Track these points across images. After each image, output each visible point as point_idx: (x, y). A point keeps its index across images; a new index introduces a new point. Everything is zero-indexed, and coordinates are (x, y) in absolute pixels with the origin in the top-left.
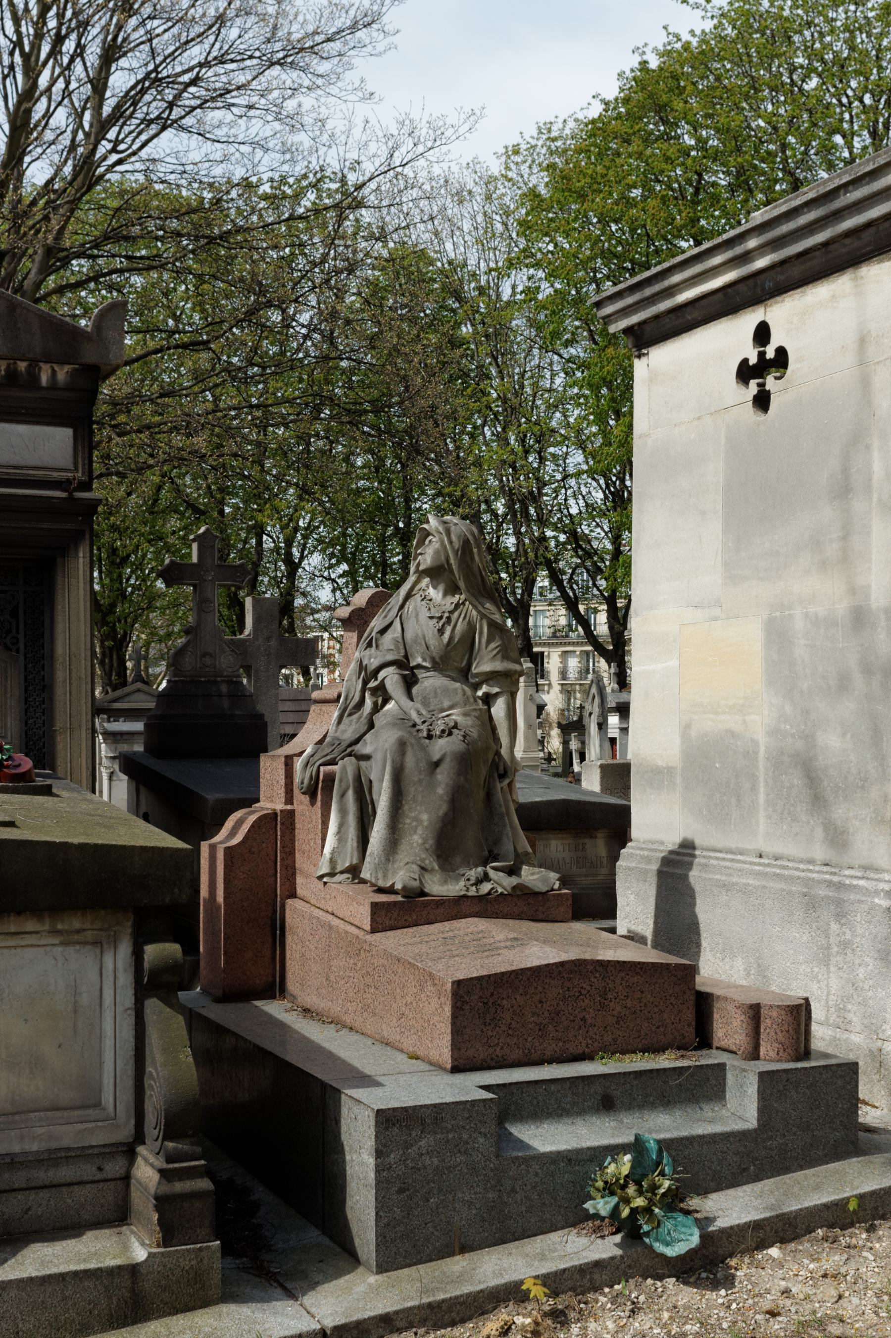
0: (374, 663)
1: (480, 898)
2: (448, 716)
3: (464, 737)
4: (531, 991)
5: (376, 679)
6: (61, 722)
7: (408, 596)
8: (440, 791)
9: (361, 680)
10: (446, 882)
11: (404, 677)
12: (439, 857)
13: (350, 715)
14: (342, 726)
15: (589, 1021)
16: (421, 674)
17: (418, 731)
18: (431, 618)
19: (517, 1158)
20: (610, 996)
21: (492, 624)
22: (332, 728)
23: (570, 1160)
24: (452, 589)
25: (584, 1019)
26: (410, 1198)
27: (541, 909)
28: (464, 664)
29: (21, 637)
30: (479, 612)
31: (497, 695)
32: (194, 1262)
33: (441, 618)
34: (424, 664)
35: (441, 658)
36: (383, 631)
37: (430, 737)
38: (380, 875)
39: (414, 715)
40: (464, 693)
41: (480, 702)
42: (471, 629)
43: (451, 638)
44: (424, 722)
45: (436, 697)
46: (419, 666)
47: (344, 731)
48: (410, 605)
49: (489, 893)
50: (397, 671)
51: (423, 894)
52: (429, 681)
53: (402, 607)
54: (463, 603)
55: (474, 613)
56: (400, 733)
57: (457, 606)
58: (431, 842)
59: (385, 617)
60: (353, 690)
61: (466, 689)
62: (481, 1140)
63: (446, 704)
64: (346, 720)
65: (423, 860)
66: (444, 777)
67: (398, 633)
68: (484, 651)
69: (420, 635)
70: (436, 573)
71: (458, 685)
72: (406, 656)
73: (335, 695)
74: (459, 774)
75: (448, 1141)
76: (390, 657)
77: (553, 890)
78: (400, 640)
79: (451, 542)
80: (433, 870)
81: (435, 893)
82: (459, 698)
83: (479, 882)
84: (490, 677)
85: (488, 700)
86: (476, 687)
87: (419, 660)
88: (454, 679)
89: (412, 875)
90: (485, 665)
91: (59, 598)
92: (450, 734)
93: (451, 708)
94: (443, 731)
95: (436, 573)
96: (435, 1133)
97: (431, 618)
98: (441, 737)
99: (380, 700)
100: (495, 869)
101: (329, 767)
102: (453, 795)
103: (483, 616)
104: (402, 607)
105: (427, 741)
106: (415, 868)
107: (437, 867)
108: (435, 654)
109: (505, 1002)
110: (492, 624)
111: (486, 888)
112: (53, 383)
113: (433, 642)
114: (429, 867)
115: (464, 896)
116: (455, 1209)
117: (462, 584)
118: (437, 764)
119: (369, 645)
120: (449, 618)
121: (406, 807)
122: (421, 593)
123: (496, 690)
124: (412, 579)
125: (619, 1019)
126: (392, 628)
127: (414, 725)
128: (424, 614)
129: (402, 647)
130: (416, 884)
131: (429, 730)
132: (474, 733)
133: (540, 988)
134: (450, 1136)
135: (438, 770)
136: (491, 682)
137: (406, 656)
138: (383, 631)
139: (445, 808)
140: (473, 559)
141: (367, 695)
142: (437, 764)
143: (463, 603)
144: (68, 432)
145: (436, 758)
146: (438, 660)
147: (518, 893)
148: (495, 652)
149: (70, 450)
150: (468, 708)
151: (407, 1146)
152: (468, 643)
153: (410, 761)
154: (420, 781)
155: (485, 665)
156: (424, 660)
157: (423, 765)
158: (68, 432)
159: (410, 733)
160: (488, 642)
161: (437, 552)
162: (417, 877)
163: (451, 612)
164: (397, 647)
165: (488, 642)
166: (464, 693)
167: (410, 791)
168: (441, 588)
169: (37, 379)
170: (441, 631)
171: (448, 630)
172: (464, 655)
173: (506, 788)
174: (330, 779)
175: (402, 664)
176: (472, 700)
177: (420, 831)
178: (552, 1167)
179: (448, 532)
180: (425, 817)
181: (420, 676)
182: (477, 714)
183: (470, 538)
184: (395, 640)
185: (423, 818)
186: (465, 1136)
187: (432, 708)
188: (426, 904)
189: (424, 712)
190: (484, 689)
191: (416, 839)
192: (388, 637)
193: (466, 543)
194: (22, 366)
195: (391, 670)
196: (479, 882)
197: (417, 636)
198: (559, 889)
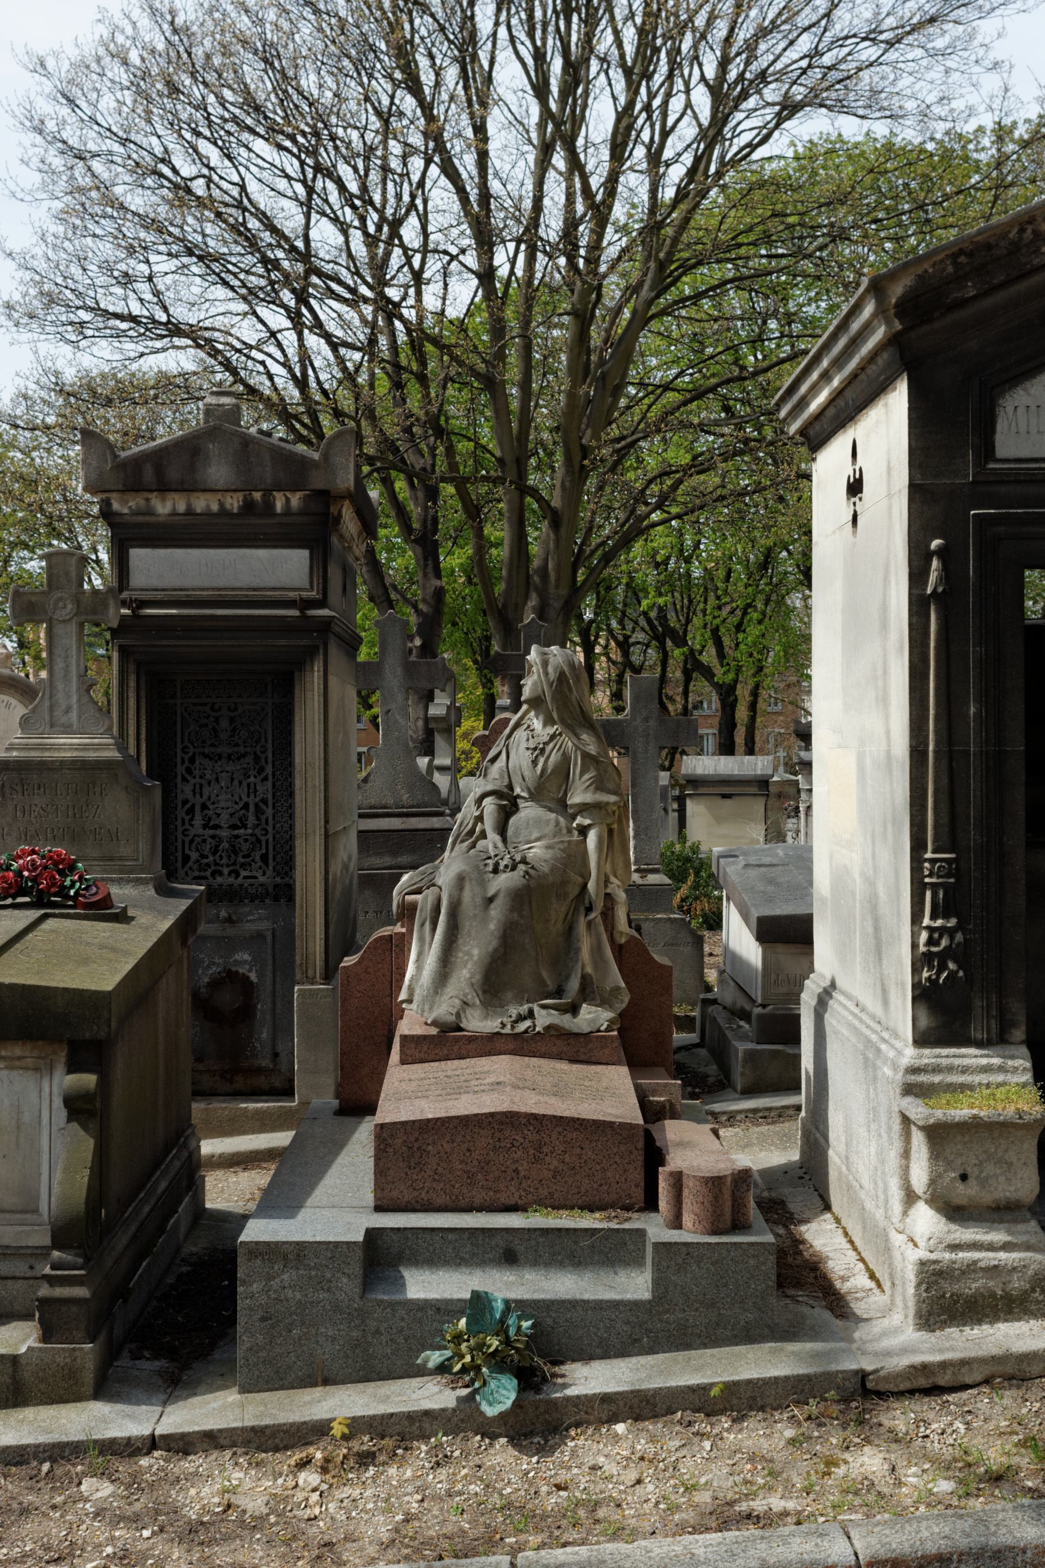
1: (516, 1036)
3: (527, 873)
4: (459, 1139)
6: (299, 827)
8: (492, 926)
10: (486, 1018)
11: (501, 808)
12: (484, 992)
13: (462, 841)
15: (522, 1174)
16: (522, 804)
19: (382, 1301)
20: (545, 1149)
21: (586, 755)
23: (438, 1309)
25: (516, 1171)
26: (272, 1327)
27: (582, 1050)
29: (269, 745)
31: (589, 826)
32: (68, 1360)
33: (535, 749)
37: (496, 871)
38: (426, 1007)
40: (557, 823)
41: (576, 833)
42: (566, 759)
43: (543, 770)
46: (518, 796)
49: (526, 1032)
51: (460, 1029)
54: (560, 734)
55: (570, 744)
56: (464, 867)
57: (553, 737)
58: (478, 977)
61: (561, 819)
62: (345, 1280)
63: (535, 835)
64: (457, 847)
65: (465, 995)
66: (497, 912)
67: (504, 764)
68: (577, 782)
70: (536, 703)
71: (553, 815)
74: (512, 910)
75: (310, 1278)
76: (490, 787)
77: (599, 1031)
79: (546, 674)
80: (474, 1005)
81: (470, 1028)
82: (550, 829)
83: (521, 1018)
84: (584, 808)
85: (583, 831)
88: (551, 810)
89: (451, 1010)
90: (577, 797)
91: (297, 710)
92: (514, 869)
93: (537, 840)
94: (506, 866)
95: (536, 703)
96: (298, 1269)
100: (544, 1007)
101: (413, 897)
102: (505, 931)
103: (577, 748)
106: (457, 1002)
107: (478, 1002)
109: (430, 1148)
110: (586, 755)
111: (522, 1026)
112: (288, 511)
113: (527, 774)
114: (470, 1002)
115: (498, 1033)
116: (317, 1343)
117: (555, 715)
118: (491, 900)
120: (543, 750)
121: (460, 942)
123: (587, 822)
124: (525, 707)
125: (556, 1173)
128: (524, 745)
130: (453, 1018)
132: (546, 869)
133: (468, 1138)
134: (313, 1273)
135: (492, 906)
137: (510, 787)
139: (495, 943)
140: (570, 690)
142: (491, 900)
143: (560, 734)
144: (305, 553)
145: (490, 894)
147: (553, 1032)
149: (307, 570)
150: (557, 840)
151: (270, 1278)
152: (563, 772)
153: (467, 895)
154: (475, 915)
155: (577, 797)
157: (479, 900)
158: (305, 553)
160: (582, 774)
161: (535, 684)
162: (454, 1012)
164: (502, 776)
165: (582, 774)
166: (557, 823)
167: (467, 925)
168: (541, 717)
169: (273, 506)
170: (535, 762)
171: (542, 760)
172: (560, 786)
173: (599, 920)
174: (413, 908)
176: (564, 831)
177: (469, 966)
178: (419, 1314)
179: (545, 664)
180: (476, 952)
181: (521, 806)
183: (566, 669)
184: (500, 768)
185: (474, 952)
186: (328, 1275)
188: (457, 1040)
190: (579, 820)
191: (465, 973)
193: (562, 674)
194: (257, 496)
196: (521, 1018)
198: (606, 1030)
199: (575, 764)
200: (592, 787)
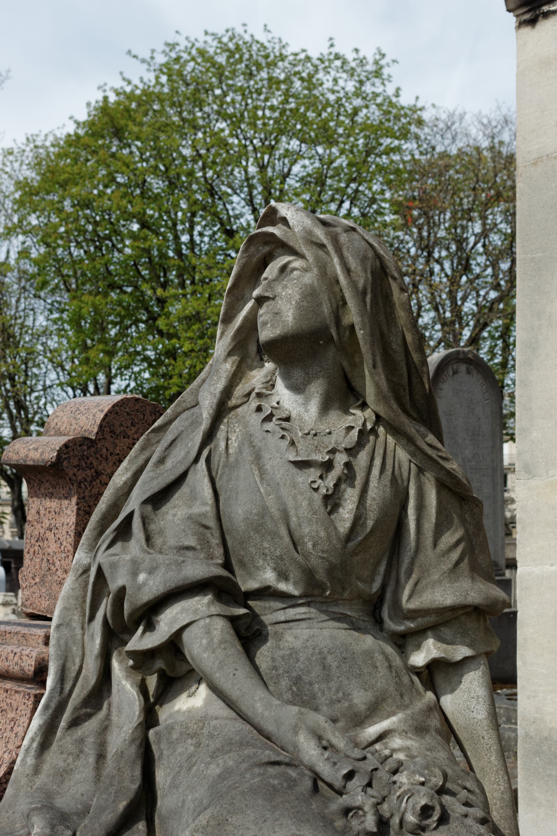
0: (150, 586)
2: (381, 737)
5: (150, 627)
7: (222, 410)
9: (97, 624)
13: (75, 723)
14: (53, 757)
16: (271, 614)
17: (347, 811)
18: (302, 465)
22: (24, 762)
24: (344, 394)
28: (376, 586)
30: (415, 450)
33: (328, 466)
34: (283, 587)
35: (331, 570)
36: (159, 499)
39: (310, 751)
44: (350, 776)
45: (327, 679)
46: (266, 593)
47: (62, 775)
48: (232, 434)
50: (216, 609)
52: (303, 635)
53: (209, 437)
54: (373, 431)
55: (402, 455)
59: (162, 461)
60: (76, 650)
63: (360, 699)
67: (204, 505)
68: (429, 554)
69: (274, 510)
72: (227, 565)
73: (29, 666)
76: (197, 569)
78: (212, 523)
86: (403, 642)
87: (269, 576)
93: (374, 711)
97: (302, 465)
99: (152, 682)
104: (209, 437)
108: (315, 562)
113: (310, 530)
119: (124, 532)
122: (254, 403)
123: (462, 652)
126: (184, 489)
128: (278, 455)
129: (215, 541)
136: (446, 632)
138: (159, 499)
141: (115, 664)
146: (321, 575)
148: (455, 555)
156: (283, 576)
163: (351, 451)
168: (317, 389)
175: (222, 588)
181: (267, 619)
192: (175, 512)
195: (201, 604)
197: (264, 512)
199: (421, 507)
200: (465, 564)
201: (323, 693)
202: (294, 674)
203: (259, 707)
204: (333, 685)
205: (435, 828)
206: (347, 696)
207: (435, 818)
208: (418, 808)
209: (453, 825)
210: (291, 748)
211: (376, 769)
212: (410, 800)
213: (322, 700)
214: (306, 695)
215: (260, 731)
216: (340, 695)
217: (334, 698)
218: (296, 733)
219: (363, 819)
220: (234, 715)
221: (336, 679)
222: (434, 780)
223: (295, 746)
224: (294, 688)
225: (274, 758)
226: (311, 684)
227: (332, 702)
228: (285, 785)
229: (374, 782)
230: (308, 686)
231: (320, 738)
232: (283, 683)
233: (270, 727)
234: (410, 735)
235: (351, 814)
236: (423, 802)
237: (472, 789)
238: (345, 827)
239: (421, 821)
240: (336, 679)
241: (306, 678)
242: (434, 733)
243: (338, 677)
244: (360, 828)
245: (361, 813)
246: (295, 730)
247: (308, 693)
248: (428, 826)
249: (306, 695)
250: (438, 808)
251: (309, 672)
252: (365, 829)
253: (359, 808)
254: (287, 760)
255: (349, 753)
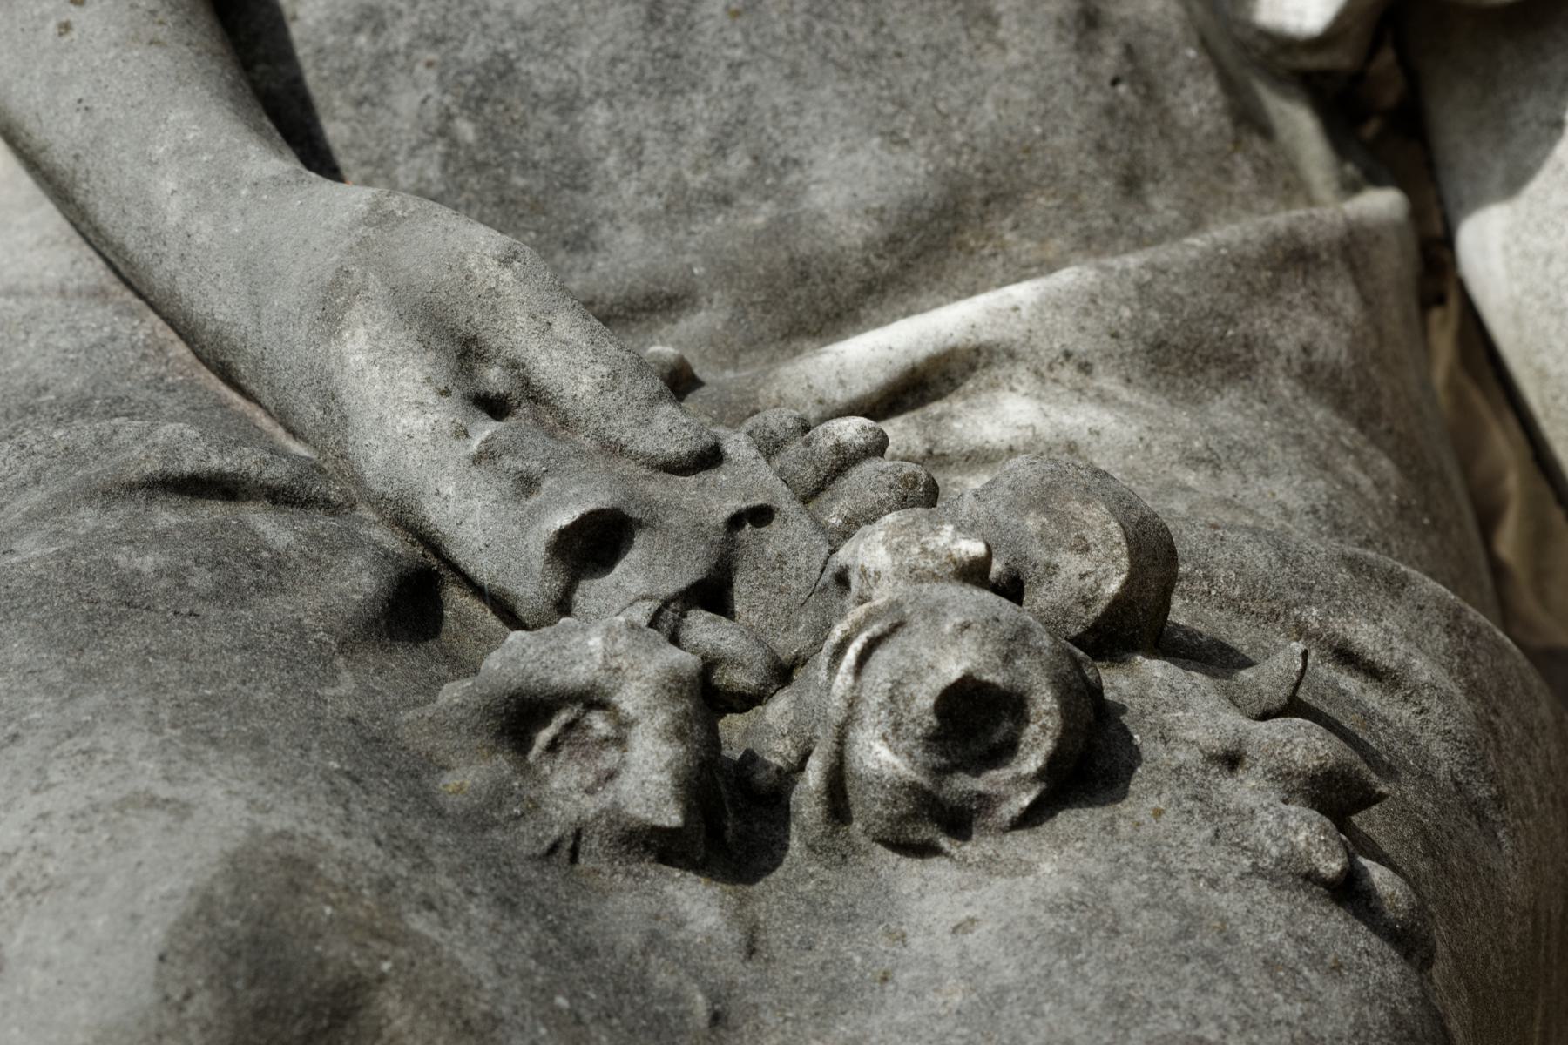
2: (913, 388)
17: (521, 717)
37: (732, 820)
39: (399, 421)
44: (594, 544)
56: (226, 810)
63: (847, 184)
92: (1093, 764)
93: (926, 246)
94: (971, 721)
98: (935, 820)
105: (697, 904)
127: (419, 597)
131: (708, 697)
159: (381, 762)
176: (1197, 102)
182: (1316, 324)
187: (628, 255)
189: (569, 362)
201: (635, 155)
202: (475, 51)
203: (170, 195)
204: (700, 112)
205: (1029, 819)
206: (774, 171)
207: (1032, 761)
208: (924, 698)
209: (1146, 804)
210: (309, 412)
211: (761, 515)
212: (882, 656)
213: (623, 192)
214: (528, 165)
215: (186, 330)
216: (737, 164)
217: (696, 181)
218: (330, 320)
219: (611, 757)
220: (93, 270)
221: (717, 77)
222: (1071, 565)
223: (330, 399)
224: (466, 130)
225: (199, 455)
226: (567, 103)
227: (682, 205)
228: (201, 579)
229: (742, 586)
230: (548, 117)
231: (468, 352)
232: (406, 102)
233: (220, 305)
234: (1107, 382)
235: (545, 736)
236: (952, 669)
237: (1385, 659)
238: (499, 794)
239: (939, 772)
240: (717, 77)
241: (541, 75)
242: (1284, 387)
243: (735, 67)
244: (591, 805)
245: (599, 724)
246: (329, 313)
247: (541, 154)
248: (987, 802)
249: (528, 165)
250: (1045, 704)
251: (562, 38)
252: (614, 814)
253: (592, 699)
254: (277, 473)
255: (623, 429)
